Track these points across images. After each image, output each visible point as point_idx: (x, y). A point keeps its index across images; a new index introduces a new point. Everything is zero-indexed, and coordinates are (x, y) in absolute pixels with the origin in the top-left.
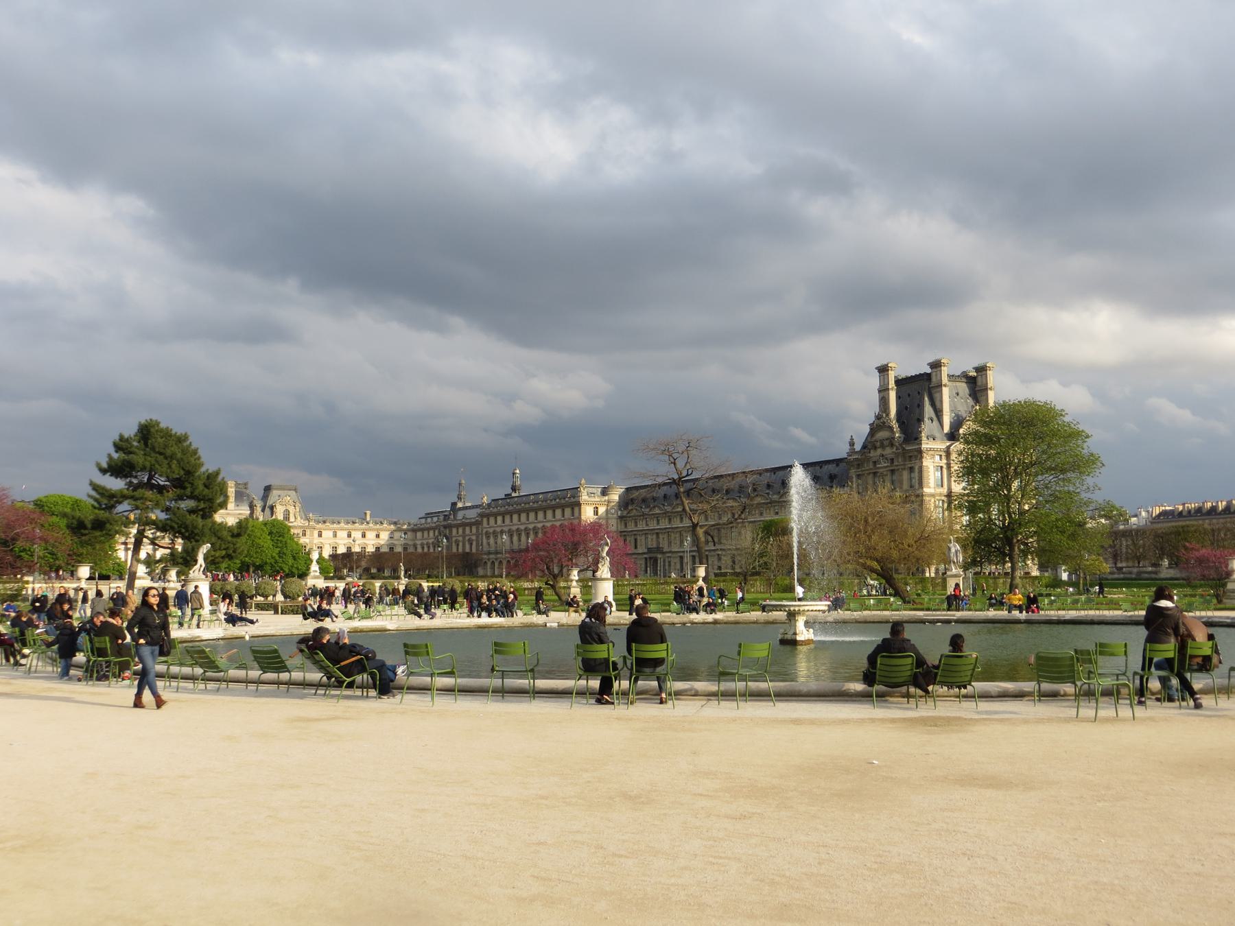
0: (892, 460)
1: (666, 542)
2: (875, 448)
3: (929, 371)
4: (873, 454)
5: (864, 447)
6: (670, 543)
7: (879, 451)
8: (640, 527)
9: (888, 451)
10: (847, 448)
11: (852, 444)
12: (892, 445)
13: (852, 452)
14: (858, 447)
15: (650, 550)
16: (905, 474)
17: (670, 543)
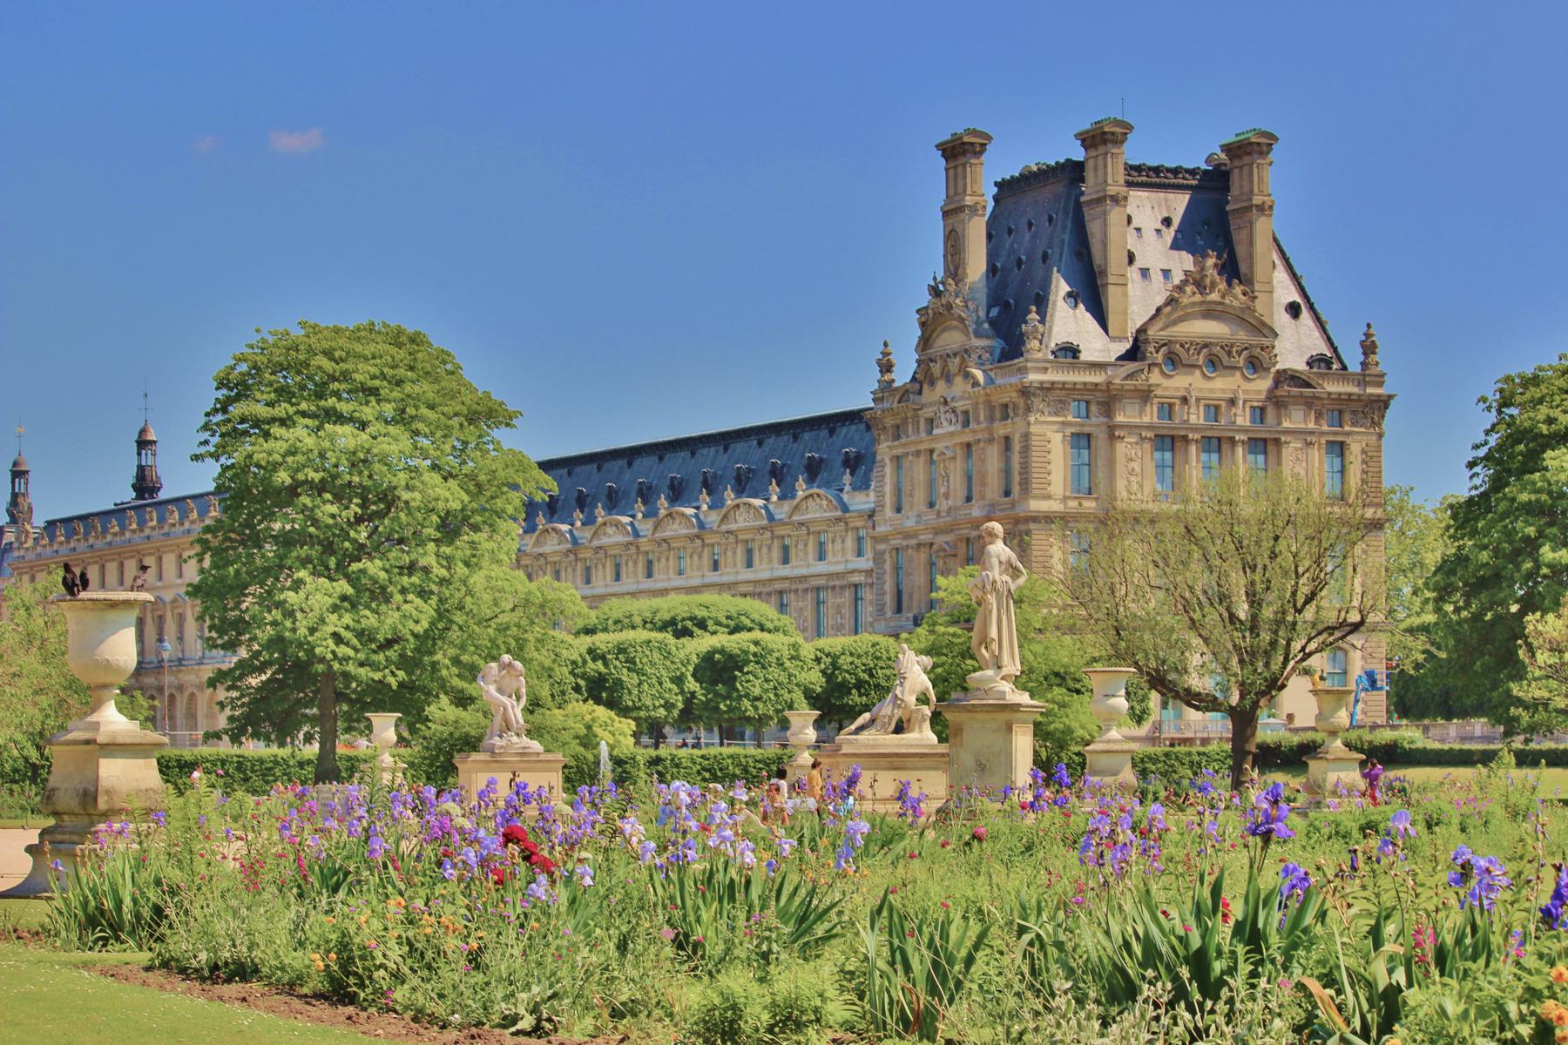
3: (1079, 154)
7: (941, 385)
10: (873, 379)
11: (886, 367)
13: (886, 388)
14: (903, 375)
16: (993, 456)
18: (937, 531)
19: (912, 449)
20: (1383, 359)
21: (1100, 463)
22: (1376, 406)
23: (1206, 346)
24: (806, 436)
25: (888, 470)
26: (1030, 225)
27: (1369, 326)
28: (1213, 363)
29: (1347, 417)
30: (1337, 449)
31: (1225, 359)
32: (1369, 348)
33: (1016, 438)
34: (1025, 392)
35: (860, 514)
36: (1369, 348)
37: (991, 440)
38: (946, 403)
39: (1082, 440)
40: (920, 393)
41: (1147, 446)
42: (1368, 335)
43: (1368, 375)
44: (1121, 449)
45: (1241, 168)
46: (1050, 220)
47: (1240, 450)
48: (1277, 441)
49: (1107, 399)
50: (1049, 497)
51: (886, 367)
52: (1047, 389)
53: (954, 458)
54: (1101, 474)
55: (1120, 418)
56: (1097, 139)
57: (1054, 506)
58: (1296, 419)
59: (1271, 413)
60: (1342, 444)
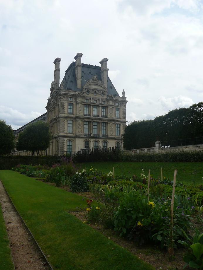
20: (126, 95)
21: (74, 108)
22: (125, 102)
27: (124, 90)
28: (96, 93)
29: (120, 104)
30: (118, 109)
31: (98, 92)
32: (124, 93)
36: (124, 93)
41: (83, 106)
42: (124, 91)
43: (124, 97)
44: (78, 105)
47: (100, 108)
48: (107, 107)
49: (76, 97)
50: (64, 114)
52: (65, 94)
54: (74, 110)
55: (78, 101)
57: (66, 115)
58: (111, 103)
59: (106, 102)
60: (119, 108)
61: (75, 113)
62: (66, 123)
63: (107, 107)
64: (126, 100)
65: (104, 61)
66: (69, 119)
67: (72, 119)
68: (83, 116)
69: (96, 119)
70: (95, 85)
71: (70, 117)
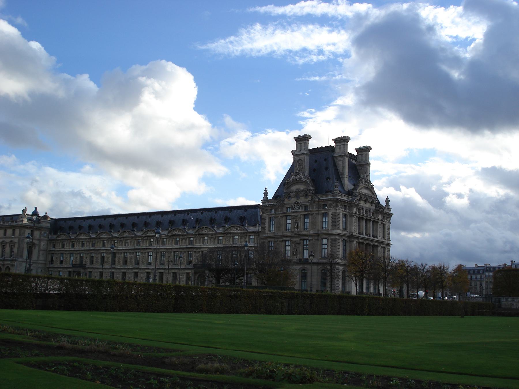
0: (306, 207)
1: (89, 260)
2: (289, 197)
3: (333, 144)
4: (286, 201)
5: (276, 196)
6: (92, 262)
7: (293, 200)
8: (66, 248)
9: (302, 200)
10: (262, 197)
11: (266, 193)
12: (306, 195)
14: (270, 197)
15: (74, 266)
16: (320, 217)
17: (92, 262)
18: (292, 237)
19: (281, 215)
23: (366, 195)
24: (220, 212)
25: (267, 221)
26: (316, 161)
31: (369, 200)
33: (330, 213)
34: (337, 201)
35: (254, 233)
37: (318, 214)
38: (298, 203)
39: (345, 215)
40: (284, 201)
45: (362, 155)
46: (325, 160)
50: (340, 229)
51: (266, 193)
52: (342, 201)
53: (300, 218)
56: (343, 141)
61: (348, 230)
62: (341, 244)
63: (377, 222)
64: (391, 212)
65: (364, 151)
66: (344, 238)
67: (346, 238)
68: (358, 235)
69: (369, 240)
70: (366, 188)
71: (345, 236)
